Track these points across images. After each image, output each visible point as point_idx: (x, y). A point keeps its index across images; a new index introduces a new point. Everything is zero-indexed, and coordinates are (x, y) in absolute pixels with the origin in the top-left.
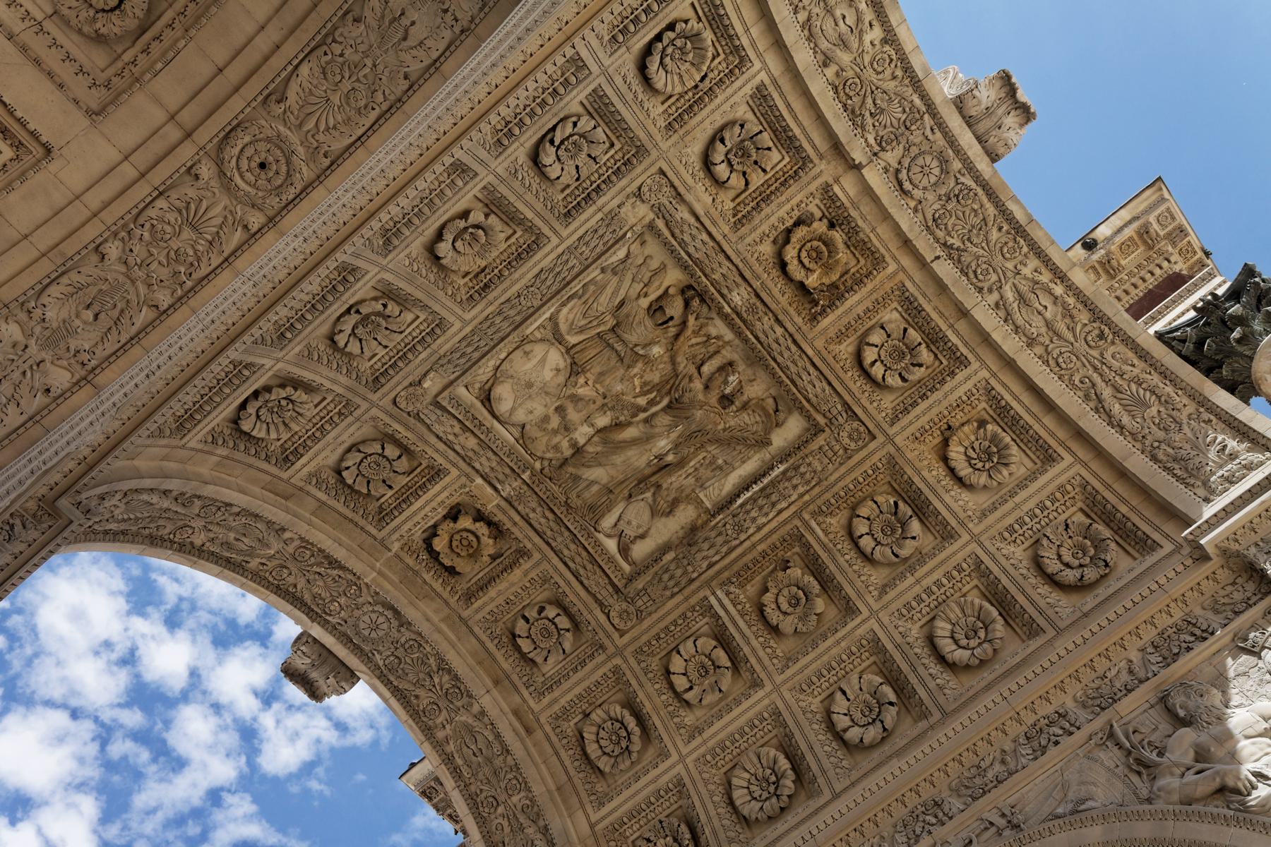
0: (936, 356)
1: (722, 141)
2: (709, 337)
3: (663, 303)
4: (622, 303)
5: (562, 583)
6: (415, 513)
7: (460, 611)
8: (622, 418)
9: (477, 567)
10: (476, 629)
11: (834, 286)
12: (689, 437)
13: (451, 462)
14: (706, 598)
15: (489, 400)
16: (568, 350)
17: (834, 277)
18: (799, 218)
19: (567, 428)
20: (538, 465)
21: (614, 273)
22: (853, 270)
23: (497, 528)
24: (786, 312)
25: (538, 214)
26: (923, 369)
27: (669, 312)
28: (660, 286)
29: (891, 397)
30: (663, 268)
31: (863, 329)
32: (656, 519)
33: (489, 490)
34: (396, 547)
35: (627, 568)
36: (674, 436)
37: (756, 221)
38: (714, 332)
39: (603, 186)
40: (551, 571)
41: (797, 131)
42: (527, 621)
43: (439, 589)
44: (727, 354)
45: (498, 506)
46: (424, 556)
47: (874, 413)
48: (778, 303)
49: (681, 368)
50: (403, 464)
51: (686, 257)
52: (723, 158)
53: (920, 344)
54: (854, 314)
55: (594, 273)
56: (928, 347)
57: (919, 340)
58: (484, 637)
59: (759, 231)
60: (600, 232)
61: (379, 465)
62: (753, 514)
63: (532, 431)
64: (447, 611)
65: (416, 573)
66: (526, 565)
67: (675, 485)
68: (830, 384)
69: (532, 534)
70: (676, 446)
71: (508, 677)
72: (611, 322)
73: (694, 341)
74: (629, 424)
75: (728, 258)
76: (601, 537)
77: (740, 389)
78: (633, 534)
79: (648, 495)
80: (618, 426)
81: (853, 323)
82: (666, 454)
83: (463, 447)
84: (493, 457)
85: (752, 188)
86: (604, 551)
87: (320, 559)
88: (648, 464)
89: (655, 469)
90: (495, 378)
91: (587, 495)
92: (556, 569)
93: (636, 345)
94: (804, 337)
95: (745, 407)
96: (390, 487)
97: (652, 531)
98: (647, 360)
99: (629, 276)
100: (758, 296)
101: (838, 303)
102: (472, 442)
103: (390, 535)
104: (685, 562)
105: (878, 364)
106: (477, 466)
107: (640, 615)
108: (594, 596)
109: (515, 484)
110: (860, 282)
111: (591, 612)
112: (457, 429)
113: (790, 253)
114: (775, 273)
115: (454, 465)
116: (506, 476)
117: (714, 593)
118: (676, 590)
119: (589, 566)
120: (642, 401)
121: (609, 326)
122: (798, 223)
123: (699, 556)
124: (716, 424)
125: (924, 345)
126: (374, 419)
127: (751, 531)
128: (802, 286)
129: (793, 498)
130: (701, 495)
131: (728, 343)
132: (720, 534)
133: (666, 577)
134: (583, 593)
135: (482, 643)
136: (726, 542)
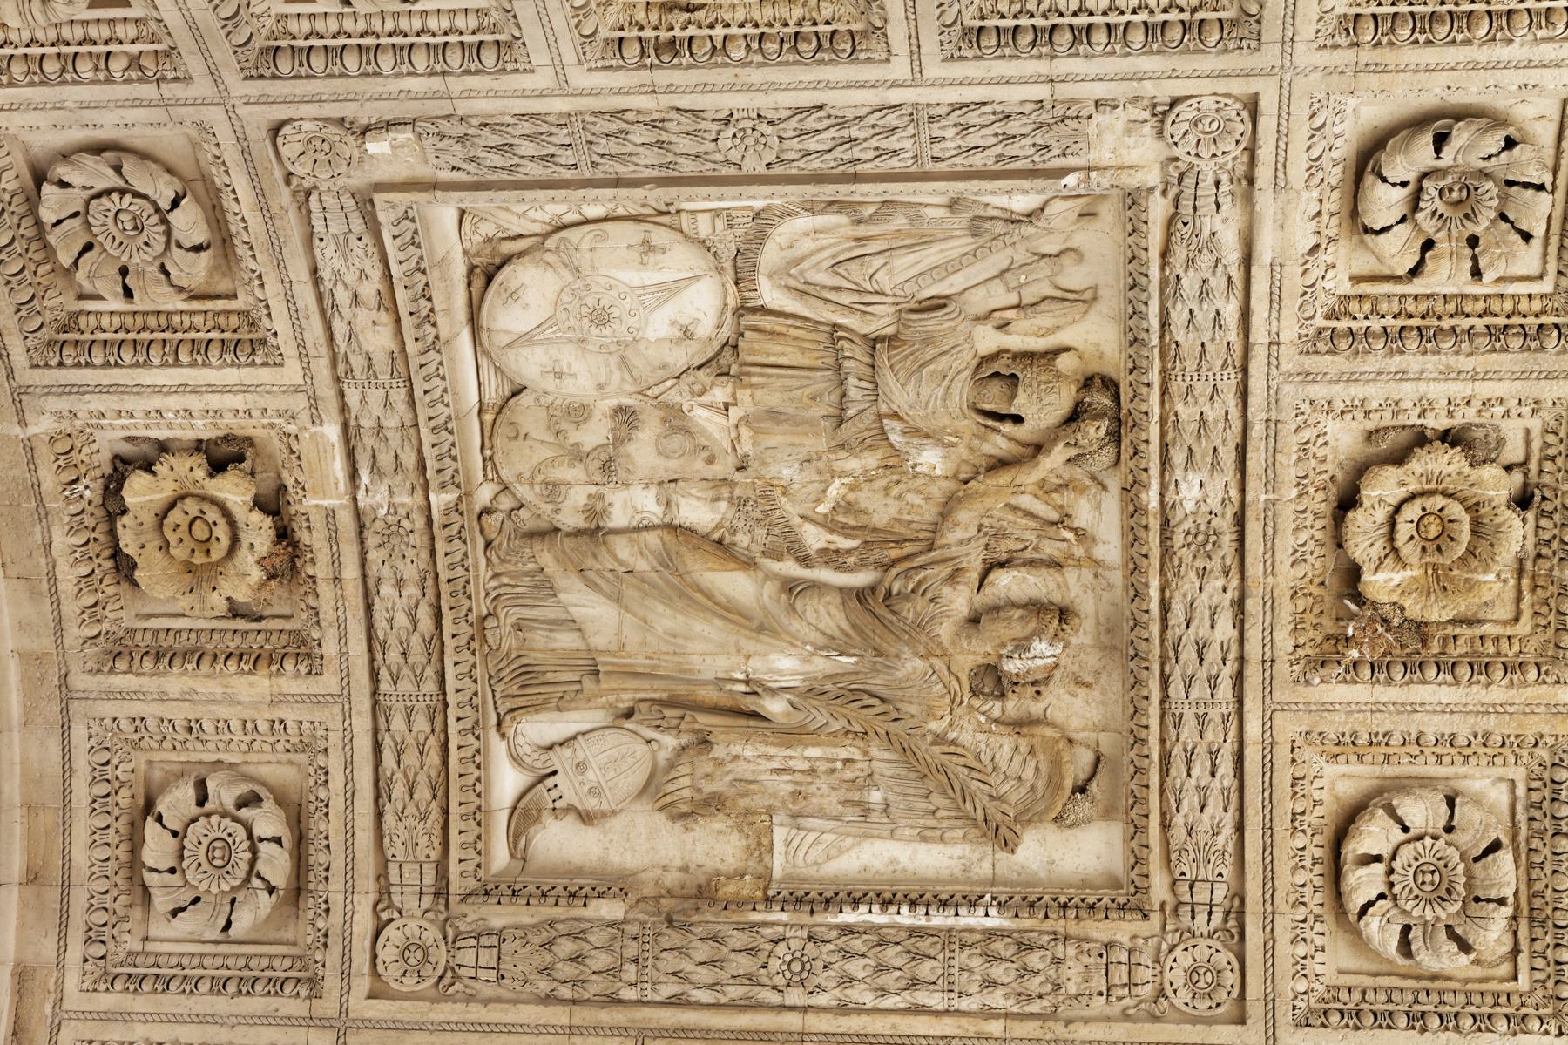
0: (1516, 951)
1: (1440, 140)
2: (1064, 520)
3: (1025, 375)
4: (937, 305)
5: (337, 780)
6: (138, 390)
7: (75, 668)
8: (742, 540)
9: (183, 604)
10: (79, 732)
11: (1421, 629)
12: (851, 695)
13: (301, 345)
15: (489, 279)
16: (743, 309)
17: (1436, 613)
18: (1467, 428)
20: (484, 495)
21: (976, 226)
22: (1488, 629)
23: (293, 558)
24: (1271, 603)
26: (1464, 959)
27: (1021, 404)
28: (1050, 331)
29: (1348, 960)
30: (1086, 299)
31: (1406, 769)
32: (645, 805)
33: (338, 467)
34: (42, 426)
35: (500, 856)
36: (822, 665)
37: (1370, 364)
38: (1083, 515)
39: (1100, 37)
40: (335, 738)
42: (202, 800)
43: (67, 586)
44: (1073, 587)
45: (331, 514)
46: (91, 491)
47: (1284, 964)
48: (1270, 570)
49: (952, 536)
50: (195, 270)
51: (1154, 323)
52: (1411, 176)
53: (1502, 902)
54: (1413, 725)
55: (931, 195)
56: (1514, 918)
57: (1508, 892)
58: (81, 763)
59: (1358, 391)
60: (1013, 127)
61: (139, 229)
62: (856, 968)
63: (527, 413)
64: (46, 643)
65: (42, 513)
66: (292, 683)
67: (741, 769)
68: (1240, 828)
69: (357, 630)
70: (812, 692)
71: (66, 886)
72: (881, 321)
73: (1026, 501)
74: (749, 564)
75: (1244, 394)
76: (498, 747)
77: (1038, 685)
78: (570, 797)
79: (670, 742)
80: (721, 547)
81: (1396, 740)
82: (773, 692)
84: (401, 407)
85: (1418, 286)
86: (479, 787)
88: (719, 682)
89: (726, 701)
91: (539, 638)
92: (348, 740)
93: (895, 415)
94: (1268, 685)
95: (1020, 725)
96: (128, 293)
97: (616, 823)
98: (894, 464)
99: (999, 260)
100: (1240, 521)
101: (1398, 673)
102: (379, 341)
103: (49, 391)
104: (632, 950)
105: (1379, 869)
106: (353, 397)
107: (447, 983)
108: (384, 863)
109: (404, 499)
110: (1482, 668)
111: (350, 891)
112: (369, 290)
113: (1383, 488)
114: (1321, 503)
115: (304, 357)
116: (398, 466)
118: (565, 992)
119: (423, 793)
120: (814, 538)
121: (870, 328)
122: (1451, 438)
123: (671, 961)
124: (930, 713)
125: (1507, 911)
126: (201, 126)
127: (821, 999)
128: (1352, 574)
129: (964, 1004)
130: (779, 834)
131: (1098, 563)
132: (751, 951)
133: (566, 947)
134: (365, 837)
135: (68, 770)
136: (751, 979)
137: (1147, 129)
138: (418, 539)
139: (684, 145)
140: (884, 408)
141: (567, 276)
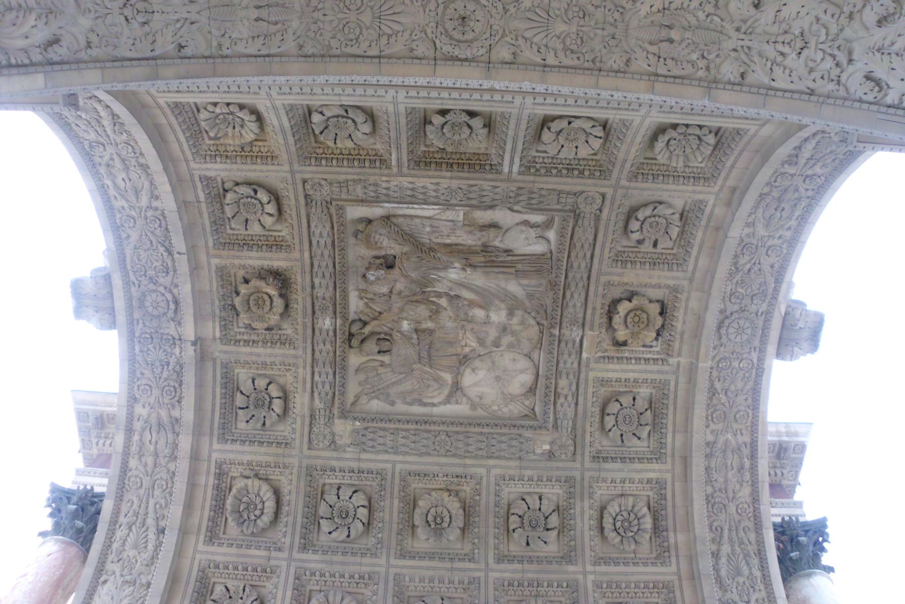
14: (519, 173)
19: (504, 329)
21: (388, 395)
24: (304, 289)
25: (392, 497)
36: (442, 274)
41: (218, 390)
69: (591, 294)
76: (553, 247)
83: (570, 385)
87: (715, 401)
90: (512, 398)
94: (303, 268)
103: (667, 373)
106: (576, 365)
112: (562, 400)
115: (587, 380)
117: (510, 172)
130: (461, 218)
137: (337, 438)
138: (565, 320)
139: (460, 445)
140: (417, 348)
141: (506, 392)
